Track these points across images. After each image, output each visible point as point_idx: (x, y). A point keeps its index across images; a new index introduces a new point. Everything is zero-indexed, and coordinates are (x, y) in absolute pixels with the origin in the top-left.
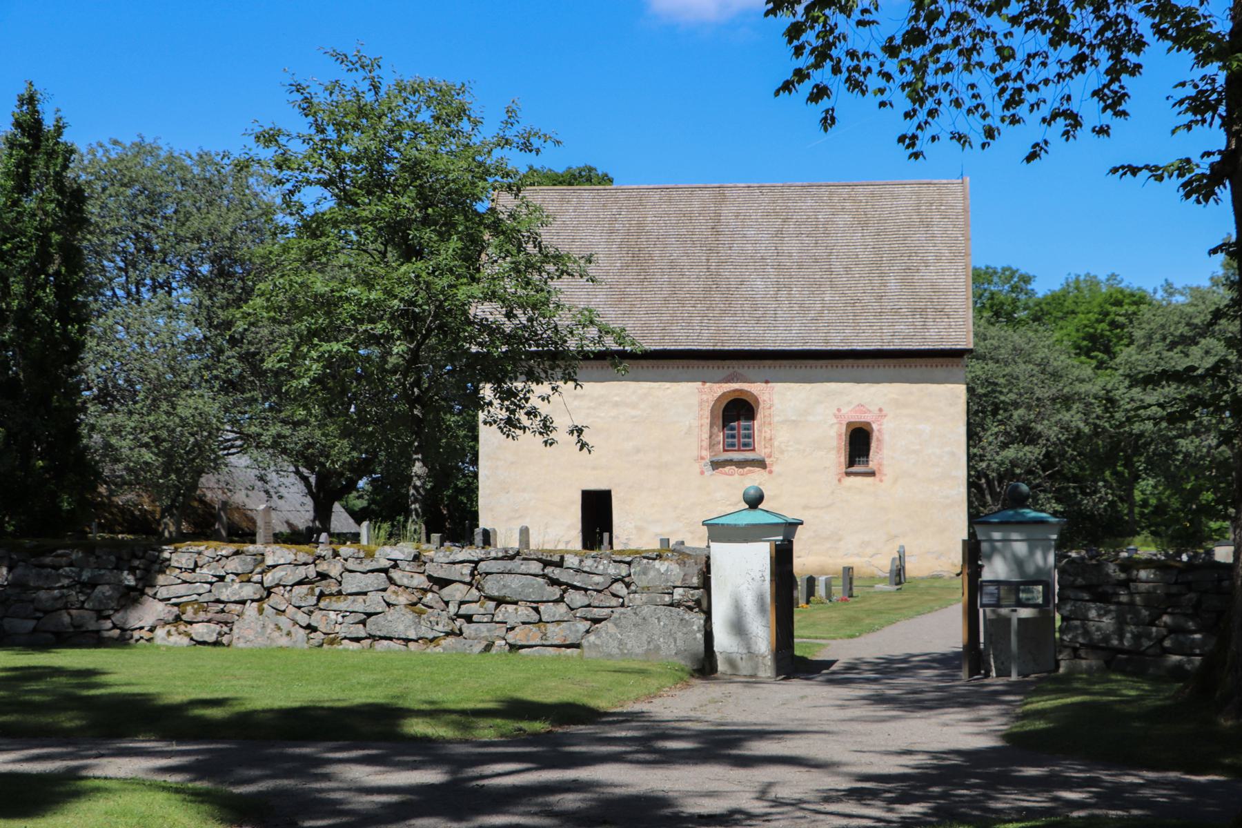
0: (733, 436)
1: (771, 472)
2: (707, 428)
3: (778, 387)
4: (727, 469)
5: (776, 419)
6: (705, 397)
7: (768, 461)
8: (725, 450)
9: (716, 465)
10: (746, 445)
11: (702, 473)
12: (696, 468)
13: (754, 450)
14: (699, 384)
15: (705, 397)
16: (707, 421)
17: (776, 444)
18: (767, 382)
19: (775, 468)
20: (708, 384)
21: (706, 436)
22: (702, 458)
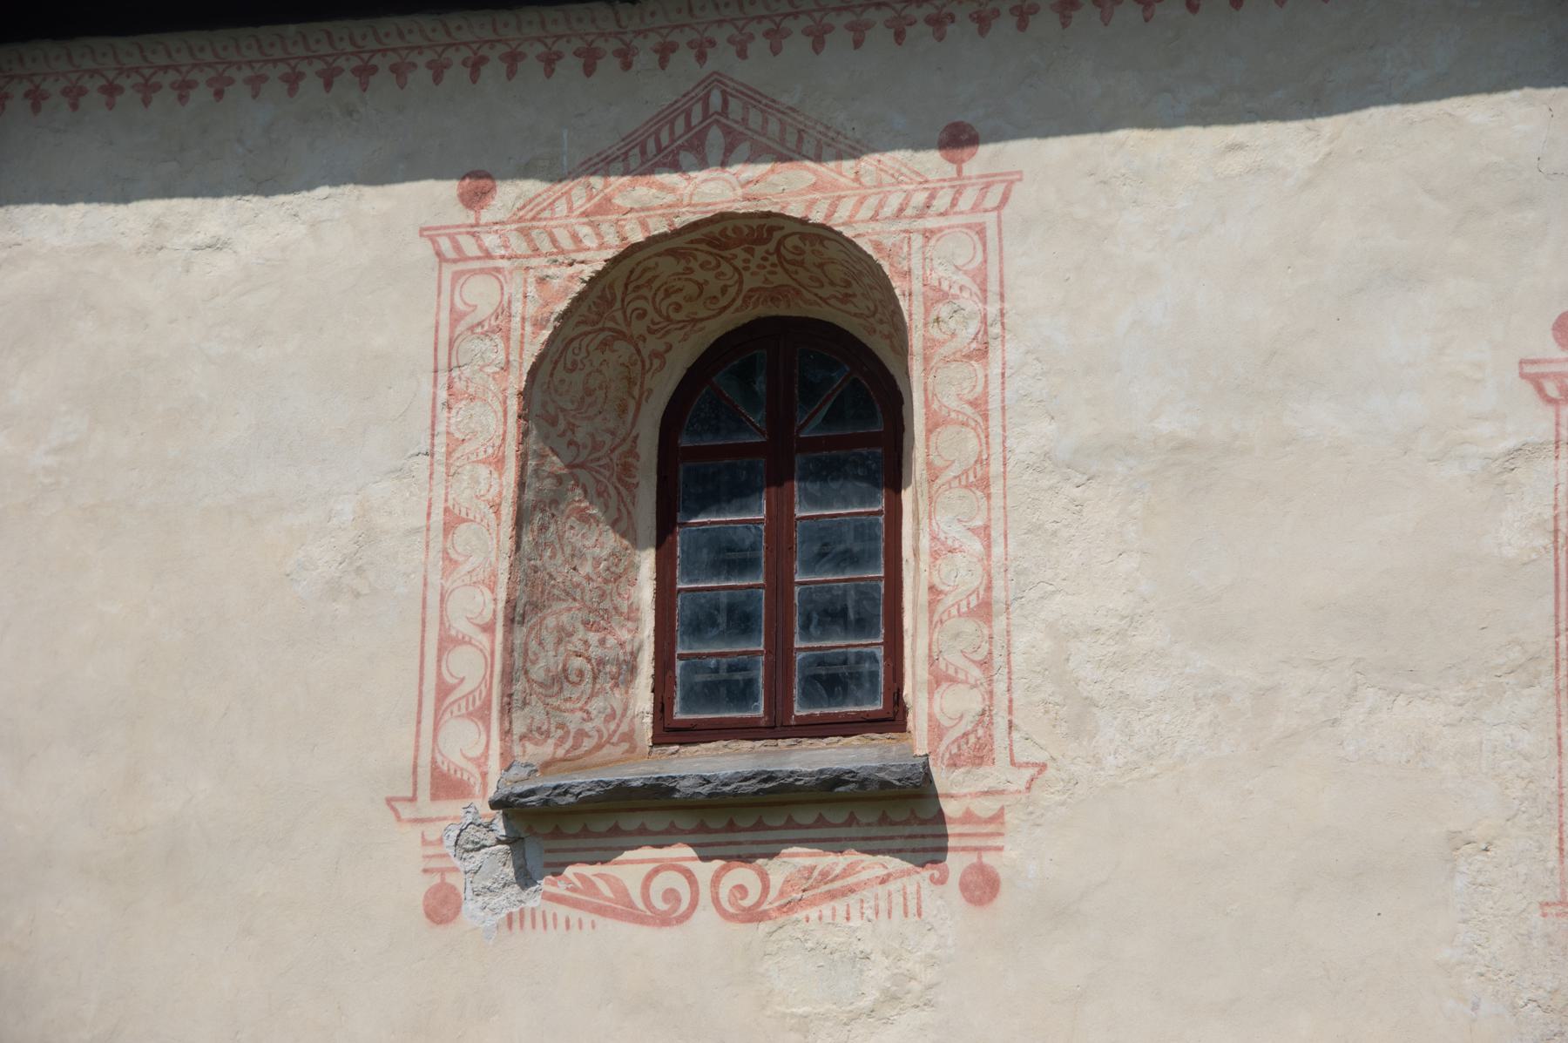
0: (740, 620)
1: (982, 888)
2: (488, 546)
3: (1045, 169)
4: (633, 868)
5: (1029, 437)
6: (481, 295)
7: (957, 792)
8: (668, 732)
9: (550, 827)
10: (833, 680)
11: (442, 907)
12: (403, 860)
13: (893, 718)
14: (436, 197)
15: (481, 295)
16: (490, 487)
17: (1028, 642)
18: (958, 139)
19: (1012, 857)
20: (510, 194)
21: (478, 604)
22: (446, 785)
